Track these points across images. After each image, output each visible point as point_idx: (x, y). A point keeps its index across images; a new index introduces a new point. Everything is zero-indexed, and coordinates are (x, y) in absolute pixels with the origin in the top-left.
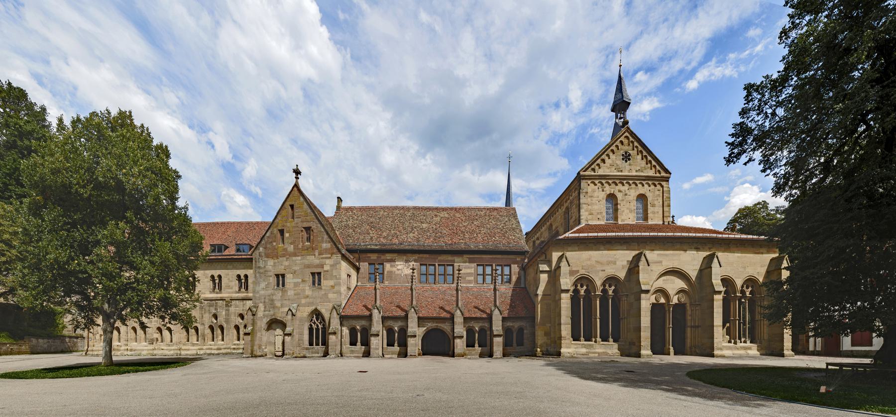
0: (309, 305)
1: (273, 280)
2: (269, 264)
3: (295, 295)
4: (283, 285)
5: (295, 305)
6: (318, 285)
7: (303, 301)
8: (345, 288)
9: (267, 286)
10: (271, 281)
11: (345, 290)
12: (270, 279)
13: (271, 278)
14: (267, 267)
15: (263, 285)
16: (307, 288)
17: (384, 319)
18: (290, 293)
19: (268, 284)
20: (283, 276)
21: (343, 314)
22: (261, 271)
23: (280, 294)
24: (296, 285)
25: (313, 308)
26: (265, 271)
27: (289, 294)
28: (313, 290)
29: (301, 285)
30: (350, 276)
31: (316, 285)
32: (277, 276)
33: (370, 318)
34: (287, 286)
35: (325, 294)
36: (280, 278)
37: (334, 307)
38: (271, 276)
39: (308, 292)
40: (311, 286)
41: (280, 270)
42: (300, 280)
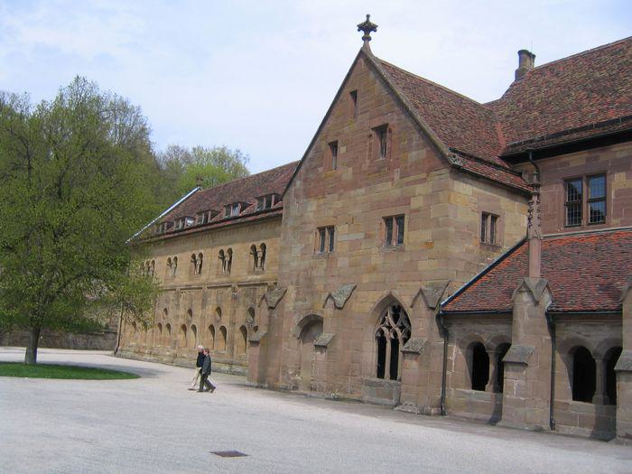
1: (314, 239)
2: (309, 209)
4: (331, 249)
7: (366, 279)
12: (308, 238)
16: (375, 250)
17: (554, 319)
18: (343, 262)
19: (305, 247)
20: (331, 229)
21: (448, 308)
23: (325, 265)
24: (354, 245)
25: (385, 293)
27: (339, 264)
30: (494, 218)
31: (394, 243)
32: (322, 230)
33: (507, 316)
34: (337, 248)
35: (412, 261)
36: (327, 231)
38: (311, 232)
39: (376, 260)
42: (361, 236)
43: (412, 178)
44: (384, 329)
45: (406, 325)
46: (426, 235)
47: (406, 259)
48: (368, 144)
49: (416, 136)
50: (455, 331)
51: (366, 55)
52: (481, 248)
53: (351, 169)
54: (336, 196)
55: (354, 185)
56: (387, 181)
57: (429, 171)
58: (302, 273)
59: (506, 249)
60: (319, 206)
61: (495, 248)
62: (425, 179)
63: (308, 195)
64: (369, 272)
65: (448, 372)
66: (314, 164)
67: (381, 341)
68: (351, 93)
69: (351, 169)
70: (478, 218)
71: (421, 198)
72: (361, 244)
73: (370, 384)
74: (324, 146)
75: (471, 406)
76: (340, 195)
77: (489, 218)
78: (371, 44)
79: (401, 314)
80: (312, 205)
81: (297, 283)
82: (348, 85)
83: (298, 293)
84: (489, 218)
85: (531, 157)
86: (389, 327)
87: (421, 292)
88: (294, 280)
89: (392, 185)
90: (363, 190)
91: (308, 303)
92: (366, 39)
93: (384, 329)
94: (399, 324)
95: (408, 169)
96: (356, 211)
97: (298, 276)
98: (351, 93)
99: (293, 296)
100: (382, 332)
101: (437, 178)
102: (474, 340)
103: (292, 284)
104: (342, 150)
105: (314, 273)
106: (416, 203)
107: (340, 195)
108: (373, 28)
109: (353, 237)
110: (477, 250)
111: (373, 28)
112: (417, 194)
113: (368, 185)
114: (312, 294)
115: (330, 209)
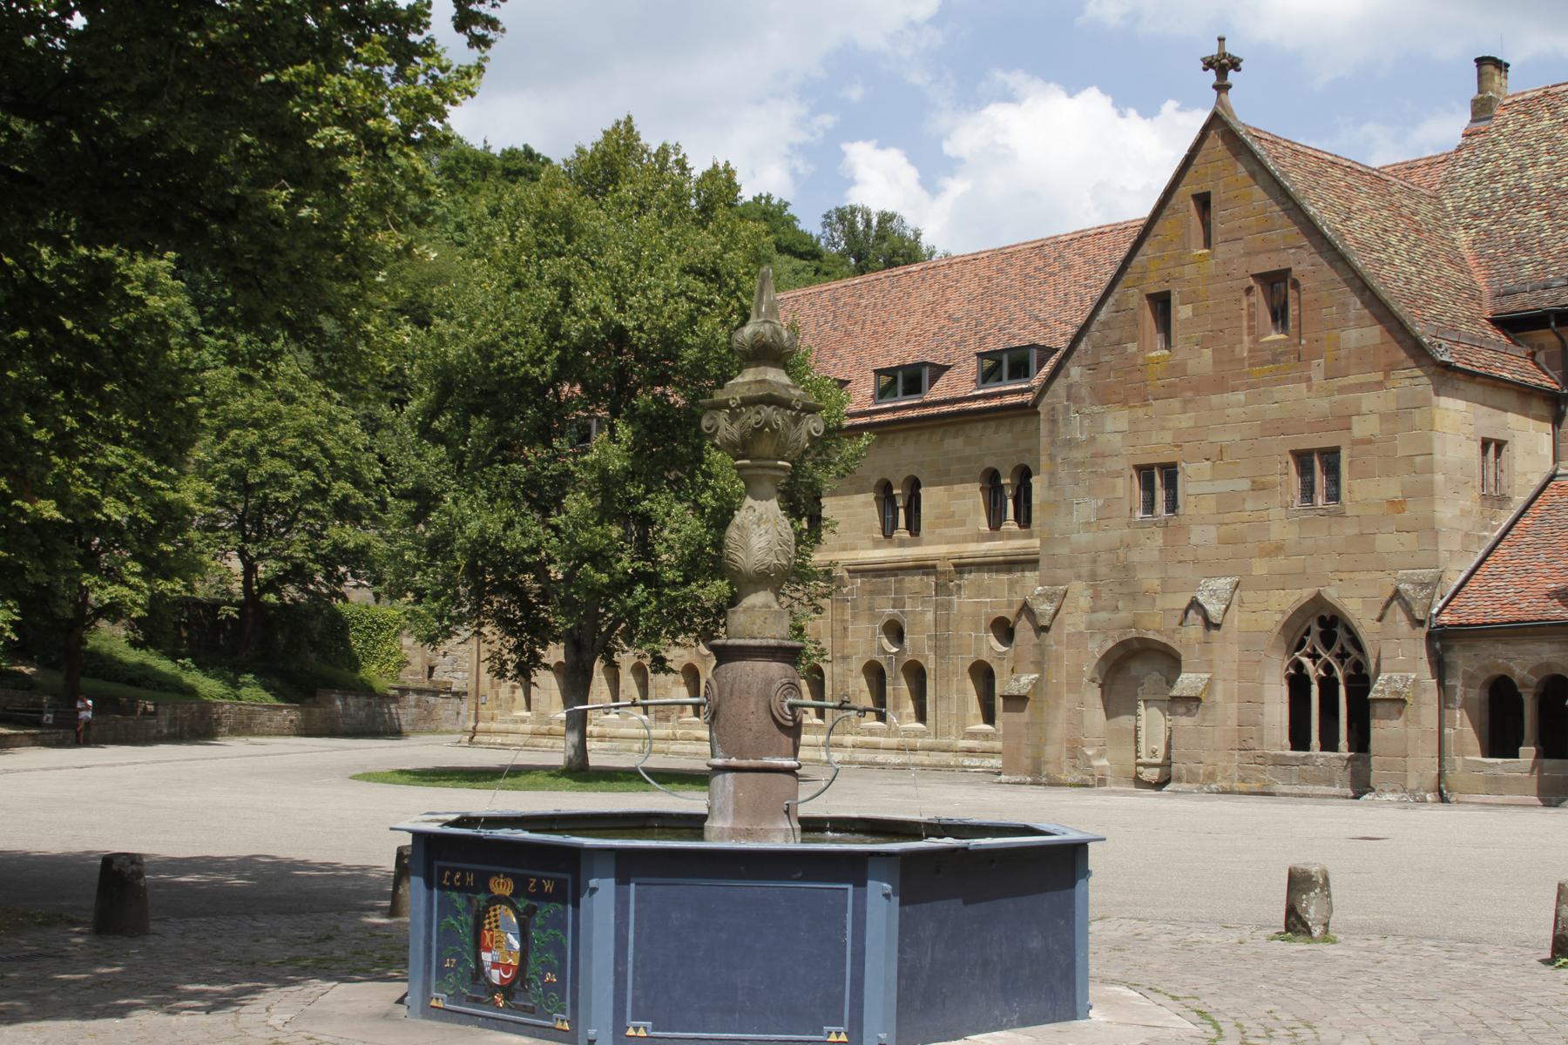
0: (1285, 580)
2: (1109, 427)
3: (1224, 541)
4: (1172, 505)
5: (1223, 584)
6: (1329, 498)
8: (1469, 500)
9: (1103, 517)
10: (1120, 492)
11: (1465, 513)
13: (1120, 482)
14: (1101, 438)
15: (1086, 509)
16: (1276, 513)
18: (1203, 536)
20: (1170, 473)
21: (1446, 619)
22: (1078, 455)
24: (1227, 502)
25: (1307, 593)
26: (1094, 456)
27: (1194, 539)
28: (1302, 522)
29: (1249, 505)
30: (1500, 445)
31: (1320, 500)
32: (1145, 474)
37: (1397, 594)
38: (1119, 474)
39: (1281, 529)
40: (1297, 502)
41: (1157, 449)
42: (1245, 485)
43: (1351, 380)
44: (1305, 660)
45: (1350, 649)
46: (1391, 488)
47: (1350, 530)
48: (1245, 304)
49: (1355, 303)
50: (1462, 660)
51: (1226, 124)
52: (1482, 505)
53: (1208, 353)
54: (1176, 403)
55: (1220, 385)
56: (1294, 381)
57: (1389, 369)
58: (1104, 556)
59: (1519, 501)
60: (1132, 422)
61: (1502, 500)
62: (1382, 382)
63: (1104, 397)
64: (1268, 554)
65: (1447, 731)
66: (1114, 335)
67: (1298, 684)
68: (1196, 197)
69: (1208, 353)
70: (1476, 448)
71: (1375, 419)
72: (1244, 500)
73: (1279, 762)
74: (1134, 297)
75: (1495, 784)
76: (1186, 402)
77: (1493, 446)
78: (1232, 97)
79: (1340, 631)
80: (1116, 421)
81: (1093, 576)
82: (1186, 179)
83: (1096, 596)
84: (1493, 446)
85: (1553, 324)
86: (1314, 656)
87: (1397, 594)
88: (1085, 570)
89: (1310, 388)
90: (1241, 396)
91: (1124, 615)
92: (1222, 87)
93: (1306, 661)
94: (1336, 648)
95: (1343, 363)
96: (1225, 438)
97: (1094, 561)
98: (1196, 197)
99: (1085, 602)
100: (1299, 666)
101: (1407, 382)
102: (1496, 672)
103: (1079, 577)
104: (1182, 312)
105: (1135, 556)
106: (1361, 428)
107: (1186, 402)
108: (1235, 64)
109: (1224, 486)
110: (1477, 508)
111: (1235, 64)
112: (1364, 409)
113: (1250, 386)
114: (1133, 596)
115: (1163, 428)
